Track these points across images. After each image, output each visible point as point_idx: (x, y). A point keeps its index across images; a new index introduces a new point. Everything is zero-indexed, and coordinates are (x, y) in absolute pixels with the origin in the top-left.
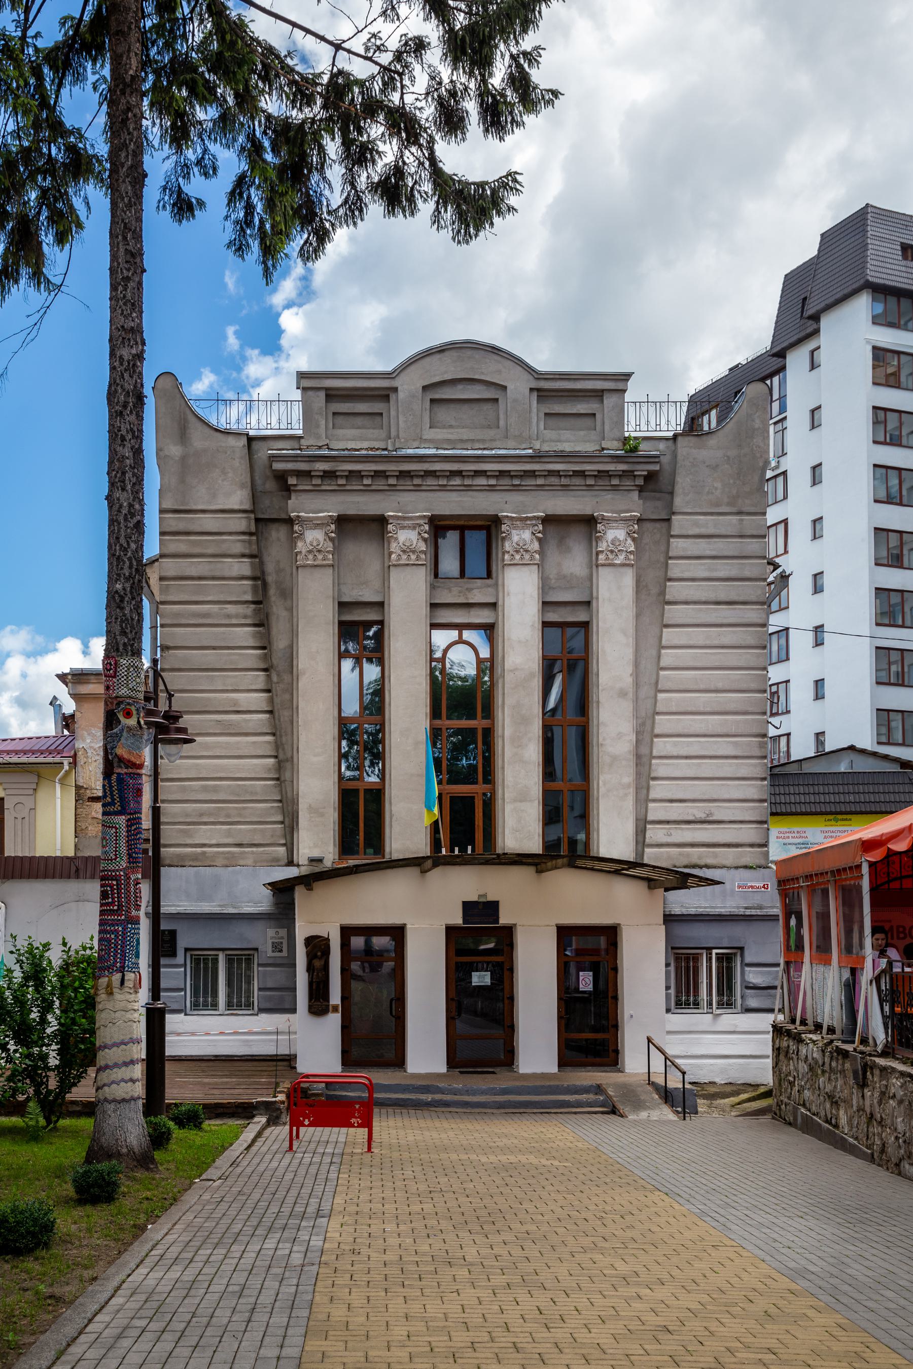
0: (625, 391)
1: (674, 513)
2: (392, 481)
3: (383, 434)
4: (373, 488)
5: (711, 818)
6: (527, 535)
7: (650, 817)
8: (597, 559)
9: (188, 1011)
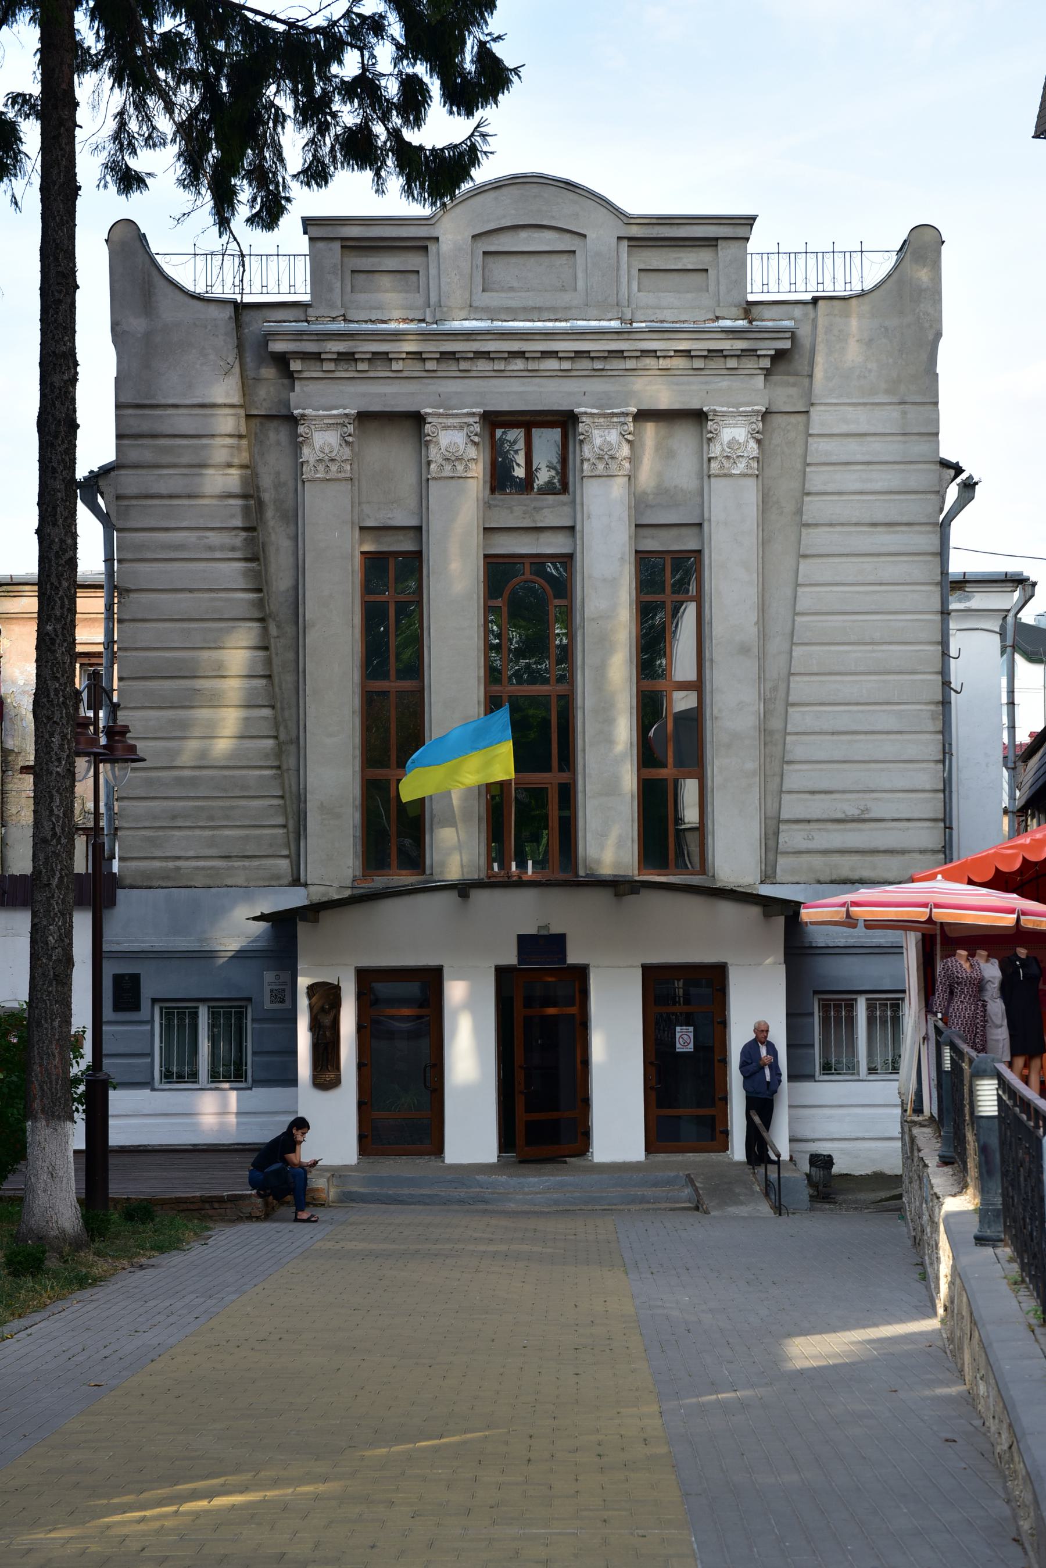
0: (747, 239)
1: (812, 404)
2: (430, 365)
3: (419, 299)
4: (405, 374)
5: (867, 816)
6: (613, 436)
7: (784, 816)
8: (709, 468)
9: (157, 1085)
